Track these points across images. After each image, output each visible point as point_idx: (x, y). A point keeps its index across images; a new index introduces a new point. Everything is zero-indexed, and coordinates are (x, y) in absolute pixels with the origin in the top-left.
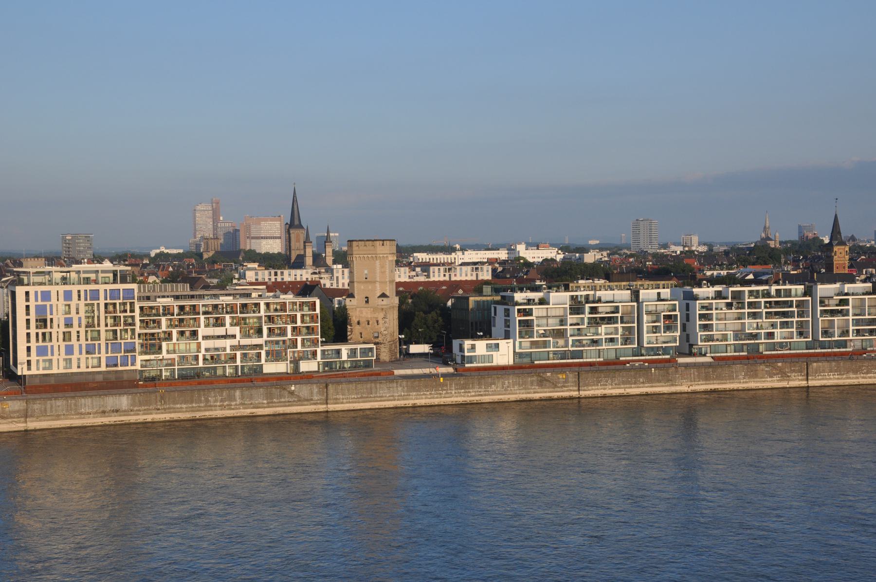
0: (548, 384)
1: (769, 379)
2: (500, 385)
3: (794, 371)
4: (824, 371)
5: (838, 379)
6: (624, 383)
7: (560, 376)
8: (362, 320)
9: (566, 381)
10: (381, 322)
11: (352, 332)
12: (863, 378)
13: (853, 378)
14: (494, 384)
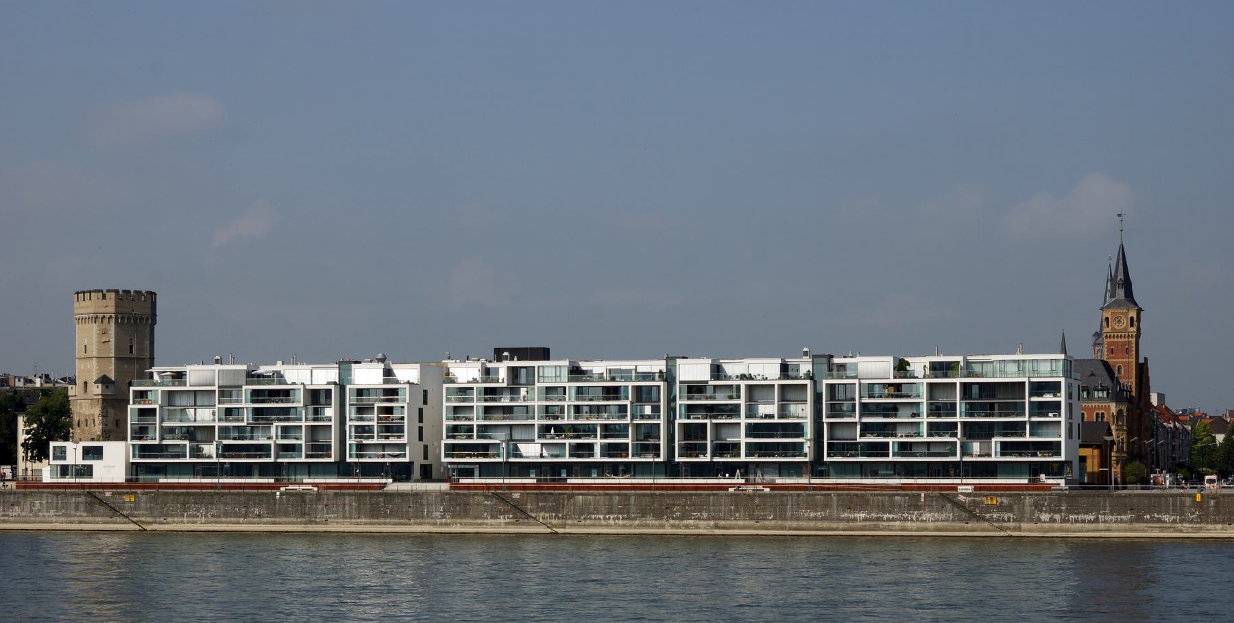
0: (102, 509)
1: (489, 521)
3: (543, 509)
4: (596, 511)
5: (624, 526)
6: (226, 515)
7: (127, 498)
8: (83, 419)
9: (136, 505)
10: (97, 421)
12: (673, 526)
13: (653, 527)
14: (18, 504)
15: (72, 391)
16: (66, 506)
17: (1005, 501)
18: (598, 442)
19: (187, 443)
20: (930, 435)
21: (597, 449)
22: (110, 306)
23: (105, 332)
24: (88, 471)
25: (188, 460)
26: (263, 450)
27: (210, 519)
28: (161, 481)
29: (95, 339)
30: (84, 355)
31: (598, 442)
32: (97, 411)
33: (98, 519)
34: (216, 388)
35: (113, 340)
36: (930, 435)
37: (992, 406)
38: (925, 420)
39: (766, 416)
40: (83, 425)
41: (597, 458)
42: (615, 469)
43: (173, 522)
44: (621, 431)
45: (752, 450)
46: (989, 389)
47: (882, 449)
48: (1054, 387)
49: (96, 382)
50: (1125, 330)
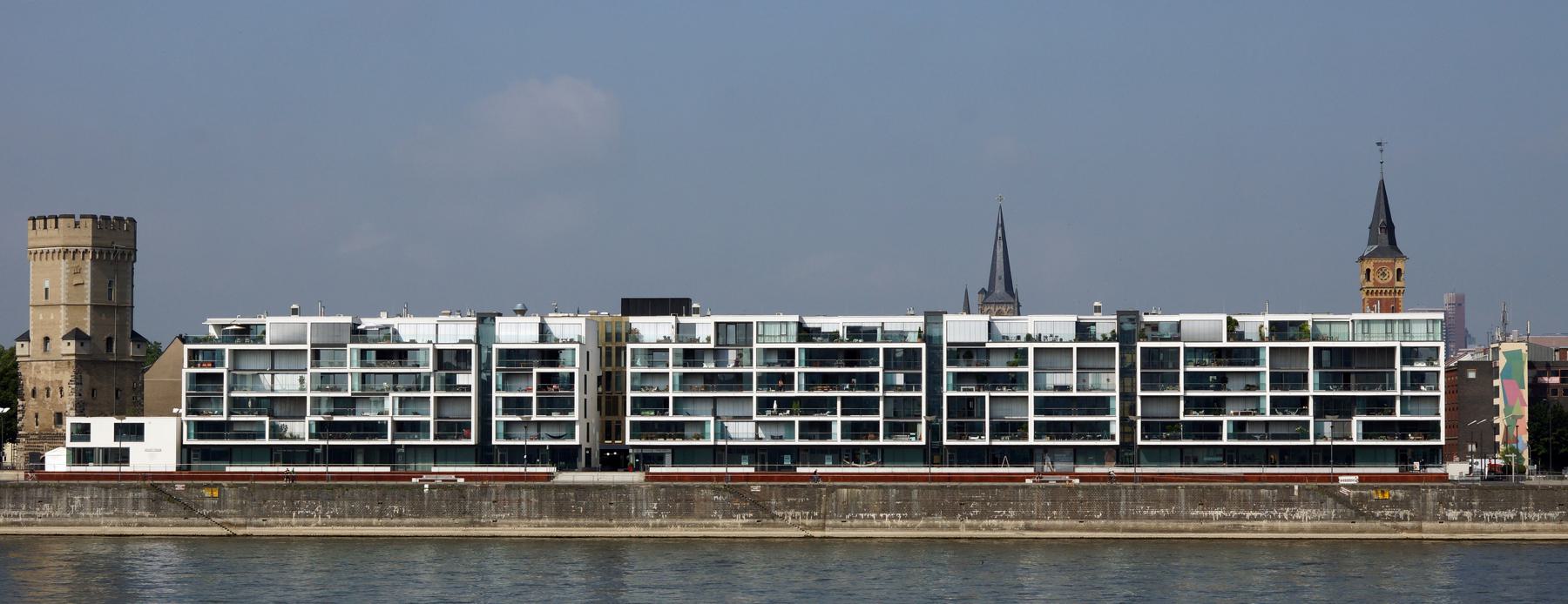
0: (172, 508)
1: (721, 522)
2: (62, 505)
3: (793, 506)
4: (867, 508)
5: (904, 528)
6: (352, 514)
7: (207, 493)
8: (40, 387)
9: (221, 502)
10: (66, 390)
11: (23, 412)
12: (969, 527)
13: (943, 528)
14: (49, 501)
15: (21, 350)
16: (119, 503)
17: (1400, 494)
18: (837, 420)
19: (266, 419)
20: (1273, 412)
21: (837, 430)
22: (84, 236)
23: (78, 272)
24: (122, 456)
25: (267, 441)
26: (376, 429)
27: (329, 519)
28: (228, 469)
29: (63, 281)
30: (44, 301)
31: (837, 420)
32: (67, 376)
33: (166, 520)
34: (308, 347)
35: (88, 282)
36: (1273, 412)
37: (1347, 376)
38: (1267, 393)
39: (1057, 388)
40: (41, 395)
41: (837, 440)
42: (853, 455)
43: (277, 524)
44: (869, 406)
45: (1042, 430)
46: (1345, 355)
47: (1213, 430)
48: (1431, 355)
49: (64, 338)
50: (1391, 284)
